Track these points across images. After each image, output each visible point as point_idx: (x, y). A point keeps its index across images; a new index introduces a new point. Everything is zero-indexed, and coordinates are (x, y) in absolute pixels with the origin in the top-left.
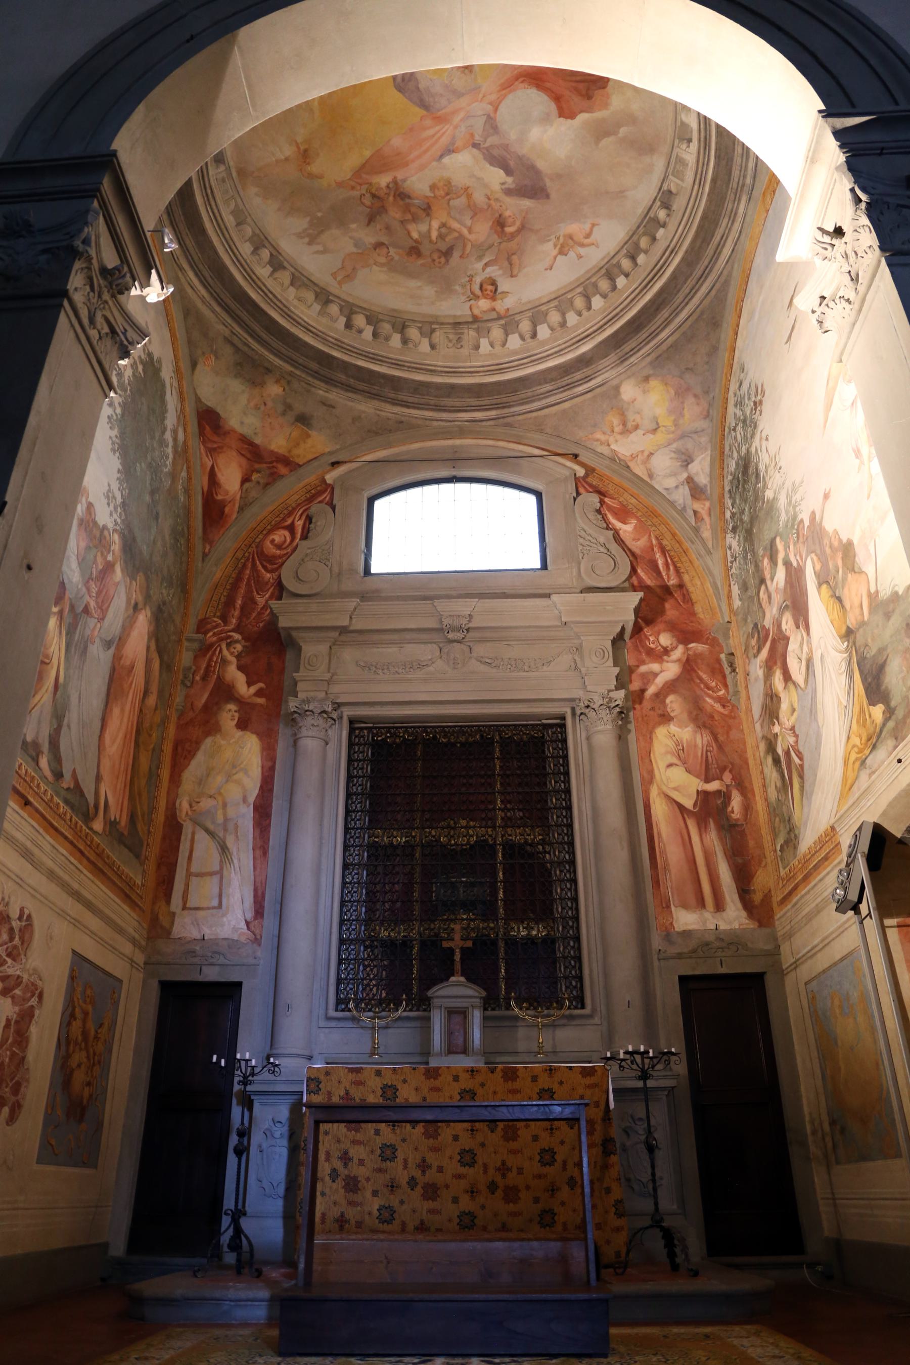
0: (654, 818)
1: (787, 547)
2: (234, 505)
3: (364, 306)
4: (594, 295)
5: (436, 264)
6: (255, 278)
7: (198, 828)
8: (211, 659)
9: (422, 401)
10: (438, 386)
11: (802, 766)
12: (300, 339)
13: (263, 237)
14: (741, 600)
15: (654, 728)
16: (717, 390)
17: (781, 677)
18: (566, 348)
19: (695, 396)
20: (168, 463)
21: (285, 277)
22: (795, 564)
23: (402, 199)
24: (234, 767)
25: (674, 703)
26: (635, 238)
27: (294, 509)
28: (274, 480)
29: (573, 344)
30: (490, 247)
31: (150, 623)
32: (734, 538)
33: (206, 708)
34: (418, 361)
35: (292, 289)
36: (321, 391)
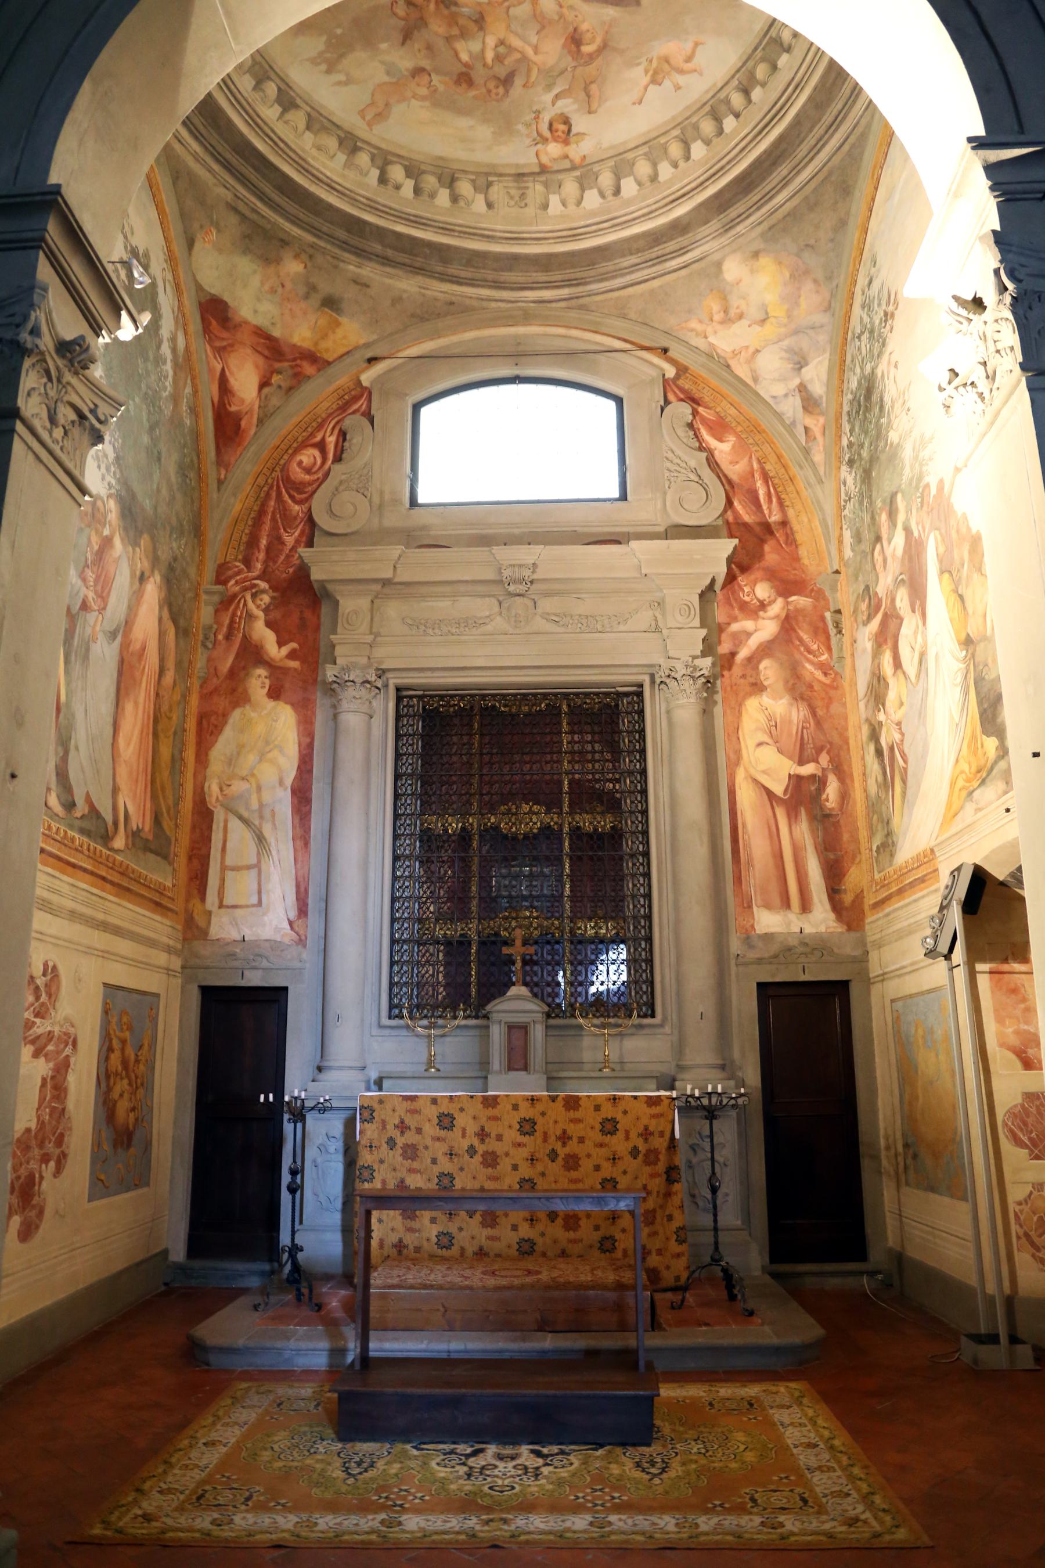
1: (909, 511)
2: (252, 415)
3: (402, 153)
4: (695, 140)
5: (493, 96)
6: (260, 122)
7: (230, 814)
8: (234, 615)
9: (478, 276)
10: (498, 257)
11: (905, 769)
12: (321, 200)
13: (267, 67)
14: (853, 550)
15: (744, 698)
16: (842, 277)
17: (891, 661)
18: (656, 210)
19: (815, 281)
20: (167, 384)
21: (298, 118)
22: (916, 534)
23: (447, 7)
24: (267, 743)
25: (769, 670)
26: (750, 64)
27: (324, 420)
28: (299, 382)
29: (666, 205)
30: (562, 72)
31: (160, 588)
32: (850, 473)
33: (232, 674)
34: (473, 224)
35: (308, 134)
36: (352, 267)
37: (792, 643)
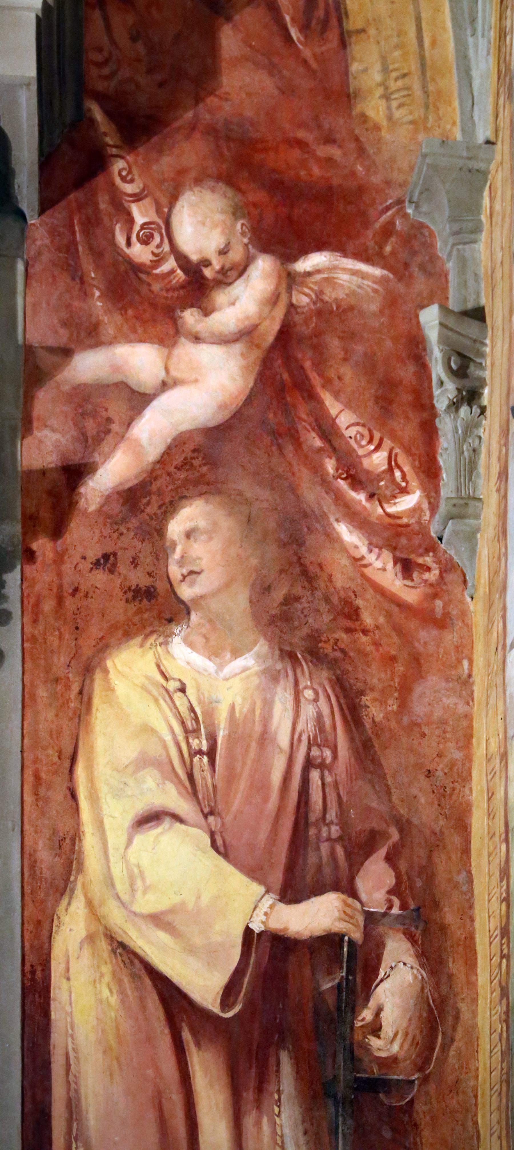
0: (57, 1037)
37: (297, 443)
